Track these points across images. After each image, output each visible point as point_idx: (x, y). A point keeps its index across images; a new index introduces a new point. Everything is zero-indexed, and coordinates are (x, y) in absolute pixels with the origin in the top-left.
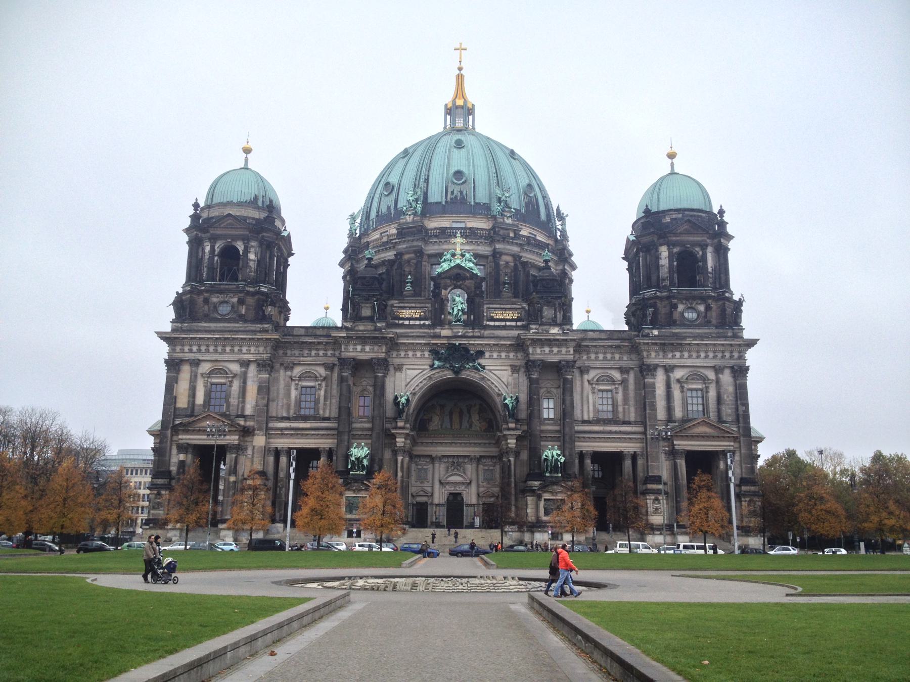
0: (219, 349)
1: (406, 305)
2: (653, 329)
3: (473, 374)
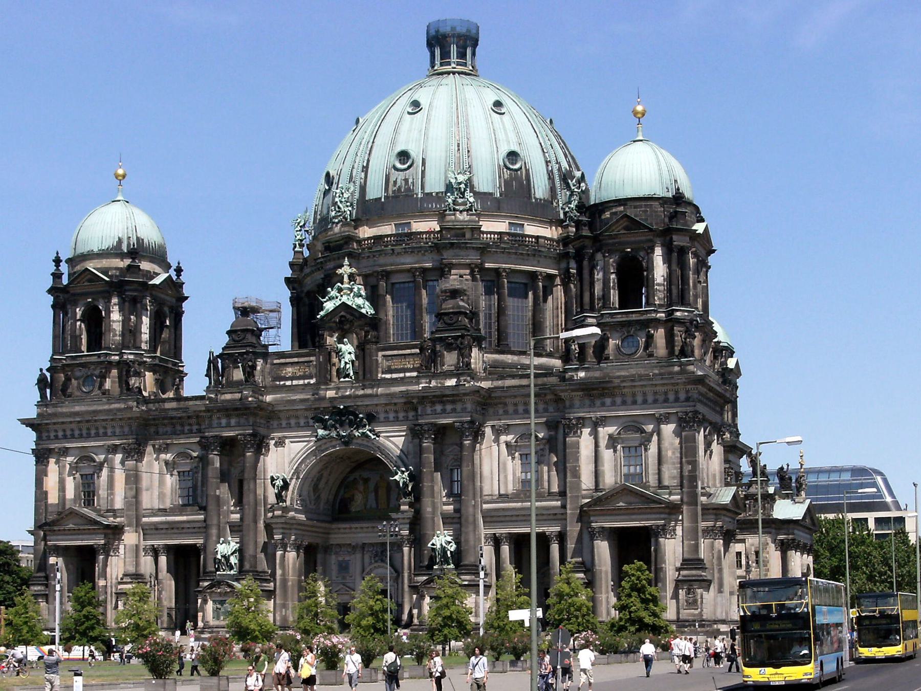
0: (84, 432)
1: (288, 360)
2: (576, 370)
3: (365, 443)
